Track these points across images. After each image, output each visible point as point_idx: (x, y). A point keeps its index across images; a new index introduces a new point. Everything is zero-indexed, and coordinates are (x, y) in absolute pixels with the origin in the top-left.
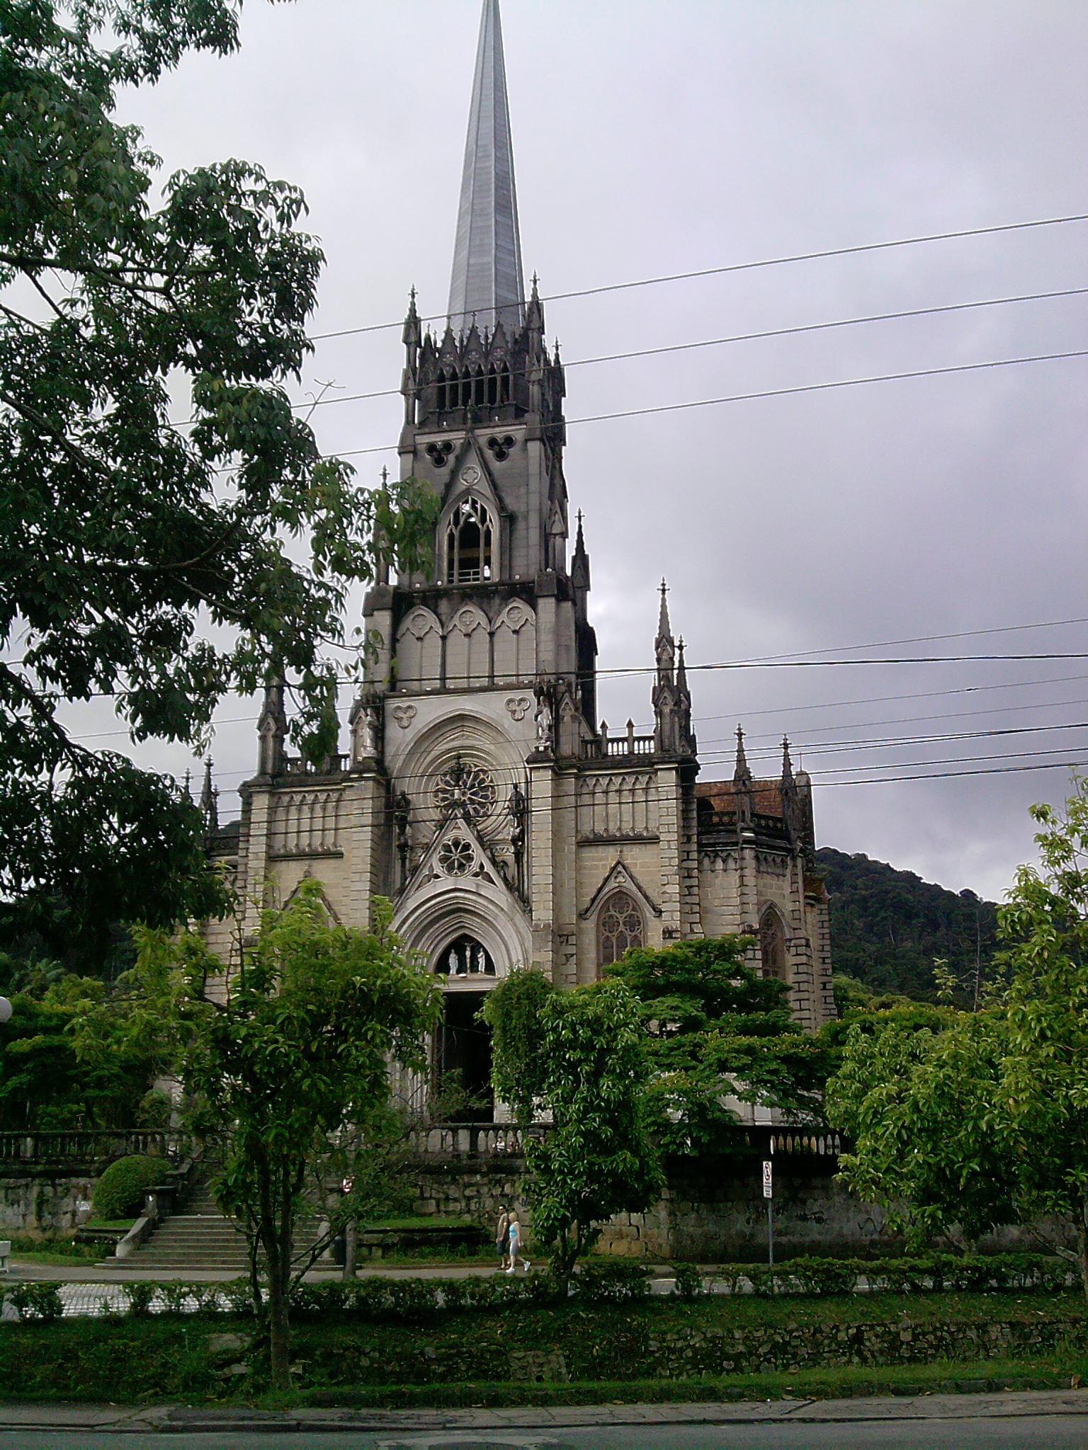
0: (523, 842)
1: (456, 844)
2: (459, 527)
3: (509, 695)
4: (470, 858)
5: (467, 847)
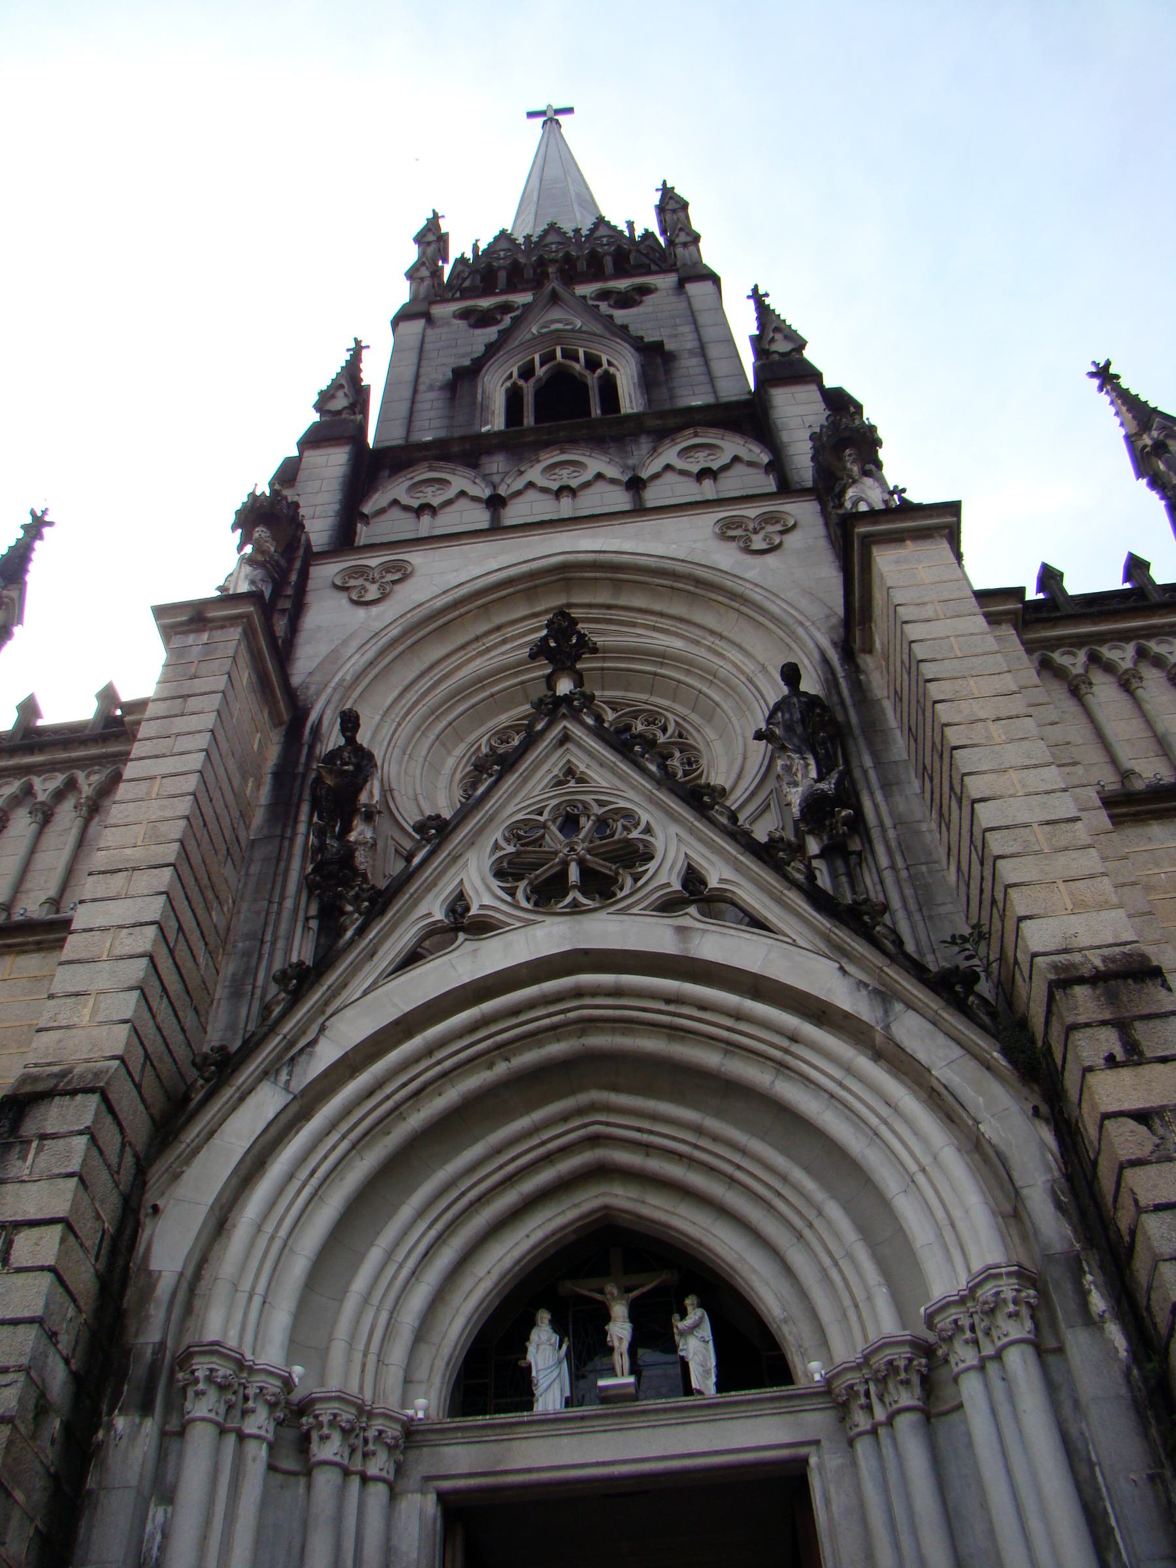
2: (532, 381)
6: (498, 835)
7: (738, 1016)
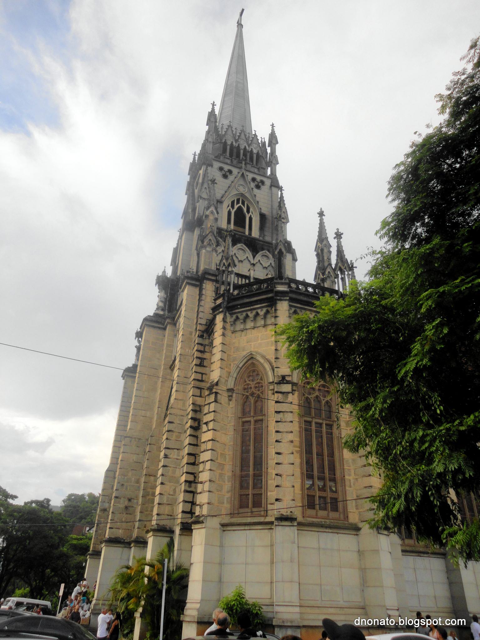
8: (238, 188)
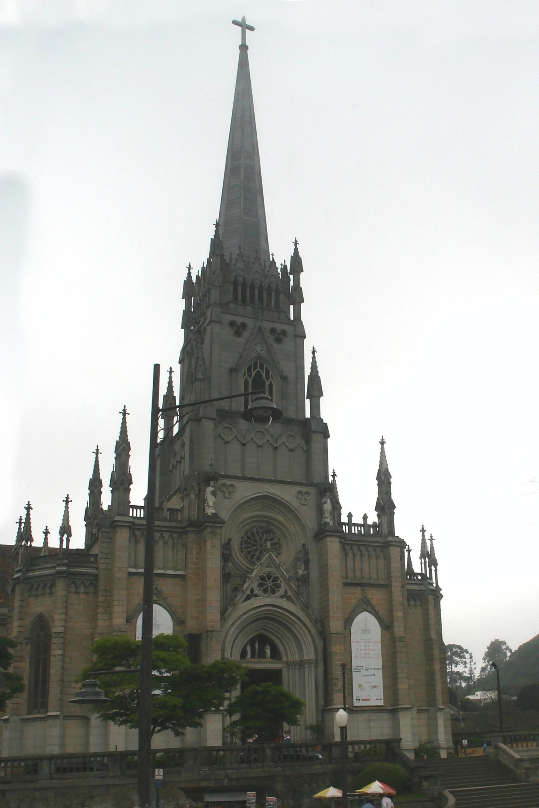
0: (309, 579)
1: (269, 577)
3: (299, 488)
4: (278, 586)
5: (276, 579)
6: (258, 578)
7: (289, 617)
8: (255, 347)
